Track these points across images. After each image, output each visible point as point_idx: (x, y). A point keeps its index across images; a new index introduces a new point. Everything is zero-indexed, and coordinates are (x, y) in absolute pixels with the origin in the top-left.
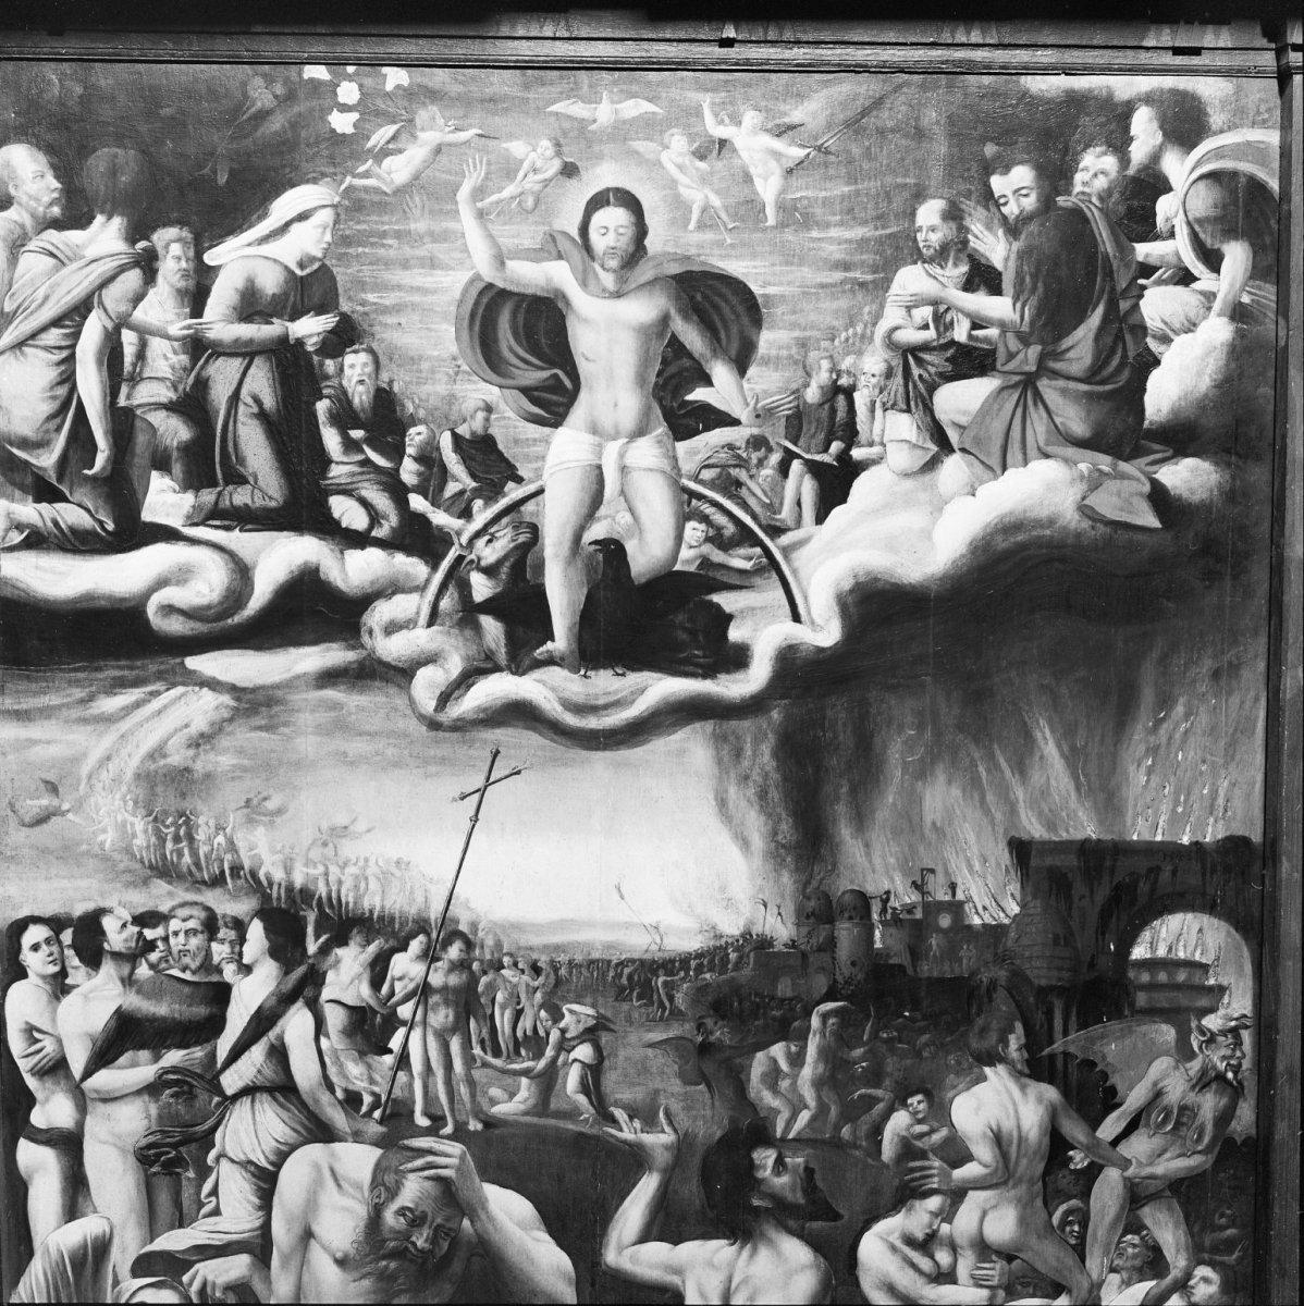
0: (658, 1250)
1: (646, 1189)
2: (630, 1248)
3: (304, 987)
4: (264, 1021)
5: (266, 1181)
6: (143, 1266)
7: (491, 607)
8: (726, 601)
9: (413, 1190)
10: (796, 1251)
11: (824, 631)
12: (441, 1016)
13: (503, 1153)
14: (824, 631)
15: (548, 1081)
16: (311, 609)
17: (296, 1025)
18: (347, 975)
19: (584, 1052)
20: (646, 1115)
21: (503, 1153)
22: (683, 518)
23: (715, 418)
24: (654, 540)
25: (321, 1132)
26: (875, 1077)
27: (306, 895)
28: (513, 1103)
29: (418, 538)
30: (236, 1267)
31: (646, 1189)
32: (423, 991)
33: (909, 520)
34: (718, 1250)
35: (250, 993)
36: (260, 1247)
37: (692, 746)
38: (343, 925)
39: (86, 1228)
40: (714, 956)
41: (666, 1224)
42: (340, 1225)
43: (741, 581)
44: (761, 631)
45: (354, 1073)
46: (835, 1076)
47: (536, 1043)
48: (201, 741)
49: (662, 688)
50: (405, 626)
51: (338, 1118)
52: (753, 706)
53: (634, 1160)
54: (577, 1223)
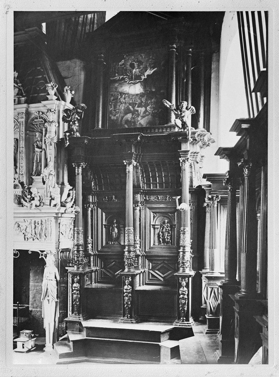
0: (137, 108)
1: (137, 105)
2: (136, 108)
3: (121, 97)
4: (120, 98)
5: (119, 106)
6: (114, 111)
7: (131, 78)
8: (141, 76)
9: (126, 106)
10: (144, 108)
11: (146, 77)
12: (128, 98)
13: (130, 104)
14: (146, 77)
15: (132, 100)
16: (123, 79)
17: (121, 98)
18: (123, 96)
19: (134, 99)
20: (137, 101)
21: (130, 104)
22: (139, 73)
23: (141, 68)
24: (138, 73)
25: (122, 104)
26: (148, 99)
27: (122, 92)
28: (131, 102)
29: (127, 75)
30: (118, 110)
31: (137, 105)
32: (127, 97)
33: (150, 72)
34: (140, 108)
35: (119, 97)
36: (119, 109)
37: (139, 83)
38: (124, 94)
39: (111, 109)
40: (140, 94)
41: (138, 107)
42: (123, 108)
43: (142, 75)
44: (143, 78)
45: (124, 101)
46: (146, 99)
47: (132, 99)
48: (117, 86)
49: (138, 81)
50: (127, 80)
51: (123, 103)
52: (142, 81)
53: (136, 104)
54: (133, 108)
